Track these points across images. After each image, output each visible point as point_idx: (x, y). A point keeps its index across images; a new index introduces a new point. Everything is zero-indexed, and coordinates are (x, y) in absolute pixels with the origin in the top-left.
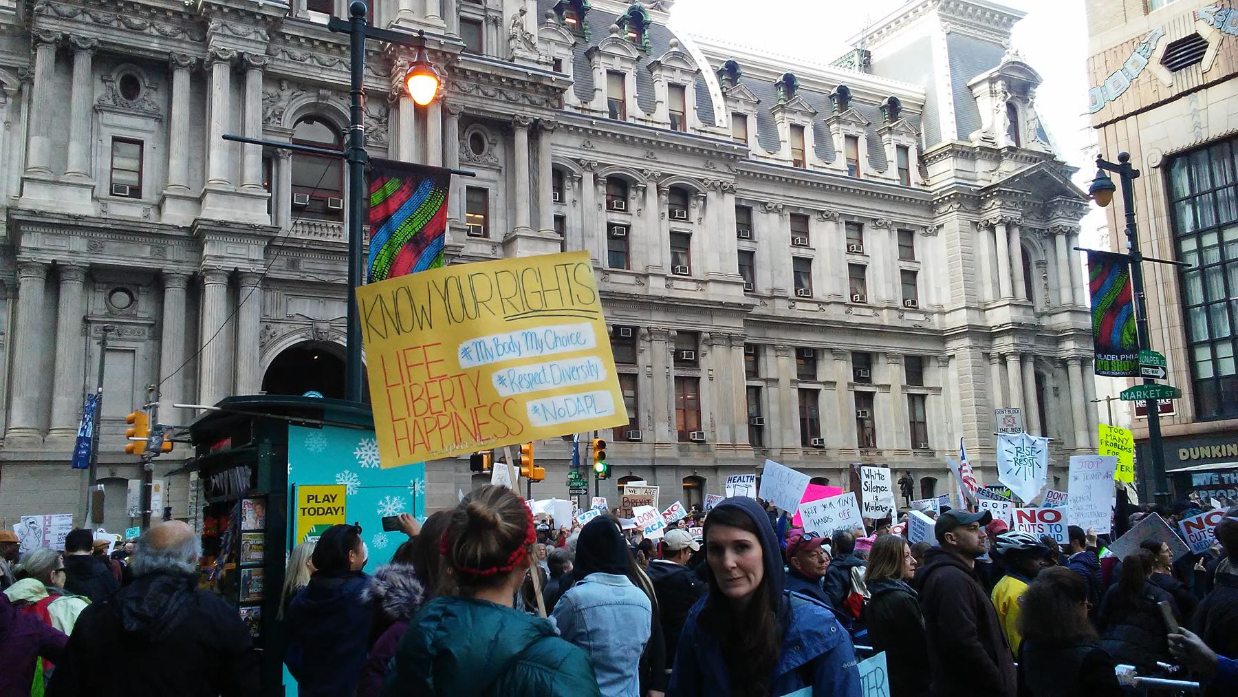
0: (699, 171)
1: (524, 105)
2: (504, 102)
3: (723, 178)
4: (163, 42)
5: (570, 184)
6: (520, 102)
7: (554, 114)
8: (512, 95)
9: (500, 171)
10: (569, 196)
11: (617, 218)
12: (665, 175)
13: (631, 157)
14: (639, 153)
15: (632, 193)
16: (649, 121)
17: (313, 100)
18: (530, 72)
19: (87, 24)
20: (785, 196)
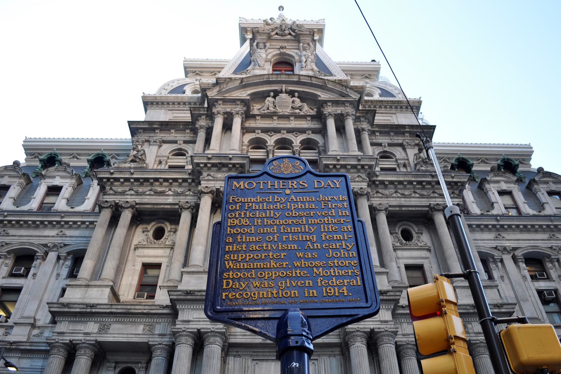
1: (435, 197)
2: (419, 198)
4: (175, 198)
5: (494, 266)
9: (429, 250)
10: (496, 274)
11: (543, 285)
13: (537, 240)
15: (549, 265)
19: (132, 195)
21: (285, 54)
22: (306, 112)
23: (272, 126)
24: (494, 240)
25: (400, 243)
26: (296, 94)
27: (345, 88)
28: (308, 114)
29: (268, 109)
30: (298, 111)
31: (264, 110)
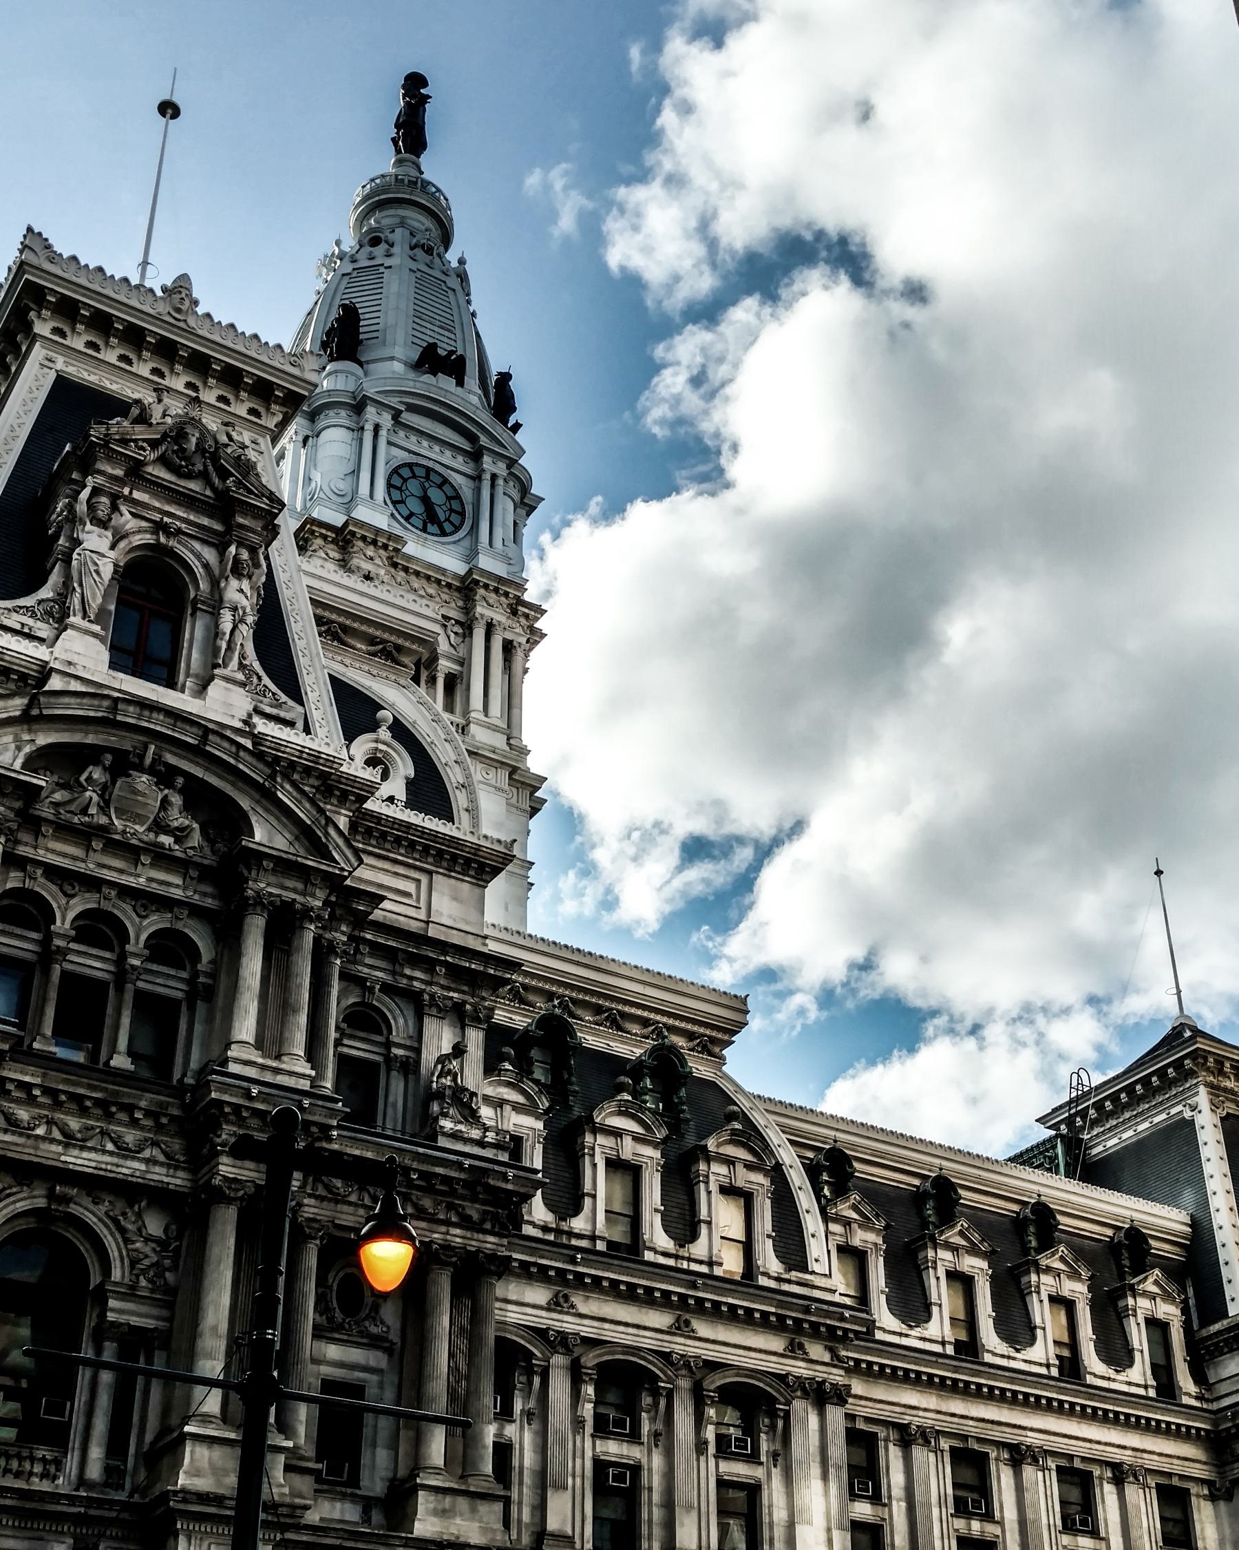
0: (774, 1358)
1: (448, 1223)
3: (820, 1373)
5: (523, 1379)
6: (442, 1216)
7: (505, 1242)
8: (427, 1203)
9: (389, 1351)
12: (713, 1366)
14: (660, 1319)
15: (647, 1400)
16: (683, 1258)
17: (41, 1203)
18: (467, 1162)
20: (939, 1412)
21: (171, 553)
22: (191, 853)
23: (80, 867)
24: (548, 1309)
25: (327, 1318)
26: (180, 781)
27: (323, 822)
28: (199, 860)
29: (84, 811)
30: (166, 840)
31: (72, 812)
